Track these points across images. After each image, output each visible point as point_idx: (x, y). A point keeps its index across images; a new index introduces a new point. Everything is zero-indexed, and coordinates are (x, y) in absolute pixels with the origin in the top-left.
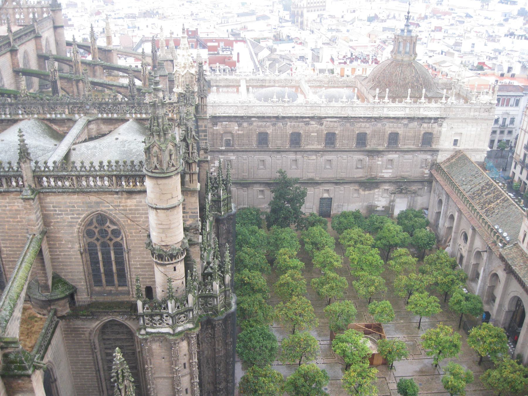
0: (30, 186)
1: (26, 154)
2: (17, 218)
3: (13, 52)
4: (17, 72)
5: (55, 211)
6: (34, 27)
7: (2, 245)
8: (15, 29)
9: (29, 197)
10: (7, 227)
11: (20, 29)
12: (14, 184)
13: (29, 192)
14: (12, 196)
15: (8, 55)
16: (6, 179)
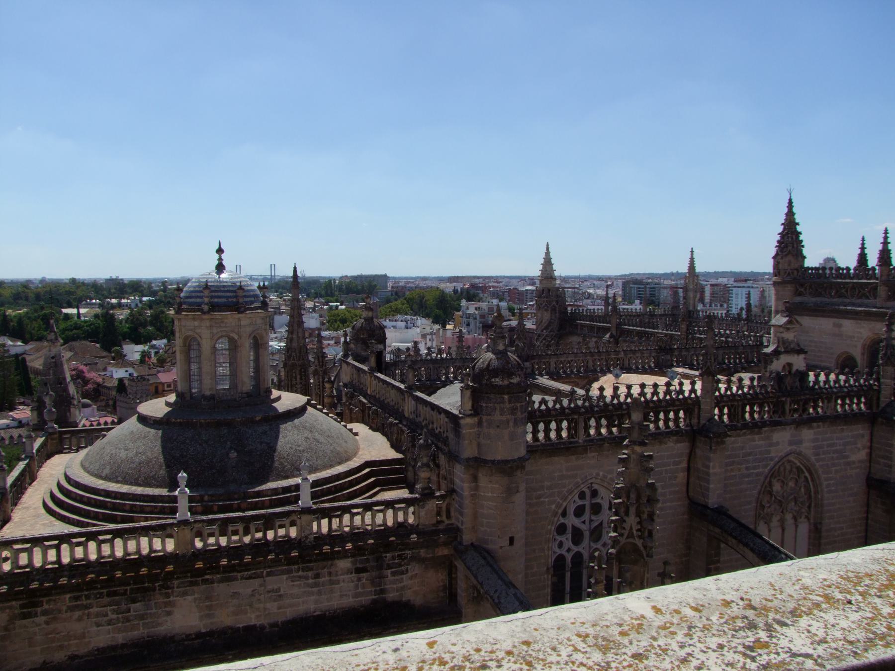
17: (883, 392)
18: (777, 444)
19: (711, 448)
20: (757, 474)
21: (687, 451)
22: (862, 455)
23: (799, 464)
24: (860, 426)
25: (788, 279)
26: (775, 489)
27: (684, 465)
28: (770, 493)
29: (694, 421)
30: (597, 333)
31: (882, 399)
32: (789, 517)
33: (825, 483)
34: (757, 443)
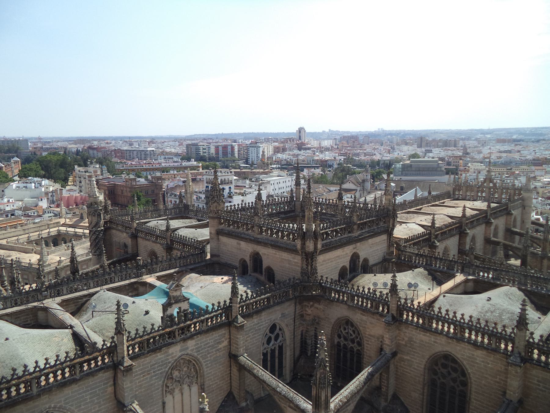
0: (520, 353)
1: (524, 323)
2: (496, 378)
3: (488, 223)
4: (487, 241)
5: (539, 385)
6: (507, 205)
7: (473, 397)
8: (493, 205)
9: (517, 363)
10: (483, 382)
11: (497, 206)
12: (503, 346)
13: (519, 360)
14: (498, 356)
15: (483, 226)
16: (497, 339)
17: (233, 311)
18: (173, 353)
19: (123, 375)
20: (161, 373)
21: (113, 375)
22: (226, 343)
23: (188, 359)
24: (223, 329)
25: (216, 216)
26: (174, 376)
27: (112, 383)
28: (172, 378)
29: (115, 359)
30: (126, 230)
31: (233, 314)
32: (186, 387)
33: (204, 364)
34: (159, 357)
